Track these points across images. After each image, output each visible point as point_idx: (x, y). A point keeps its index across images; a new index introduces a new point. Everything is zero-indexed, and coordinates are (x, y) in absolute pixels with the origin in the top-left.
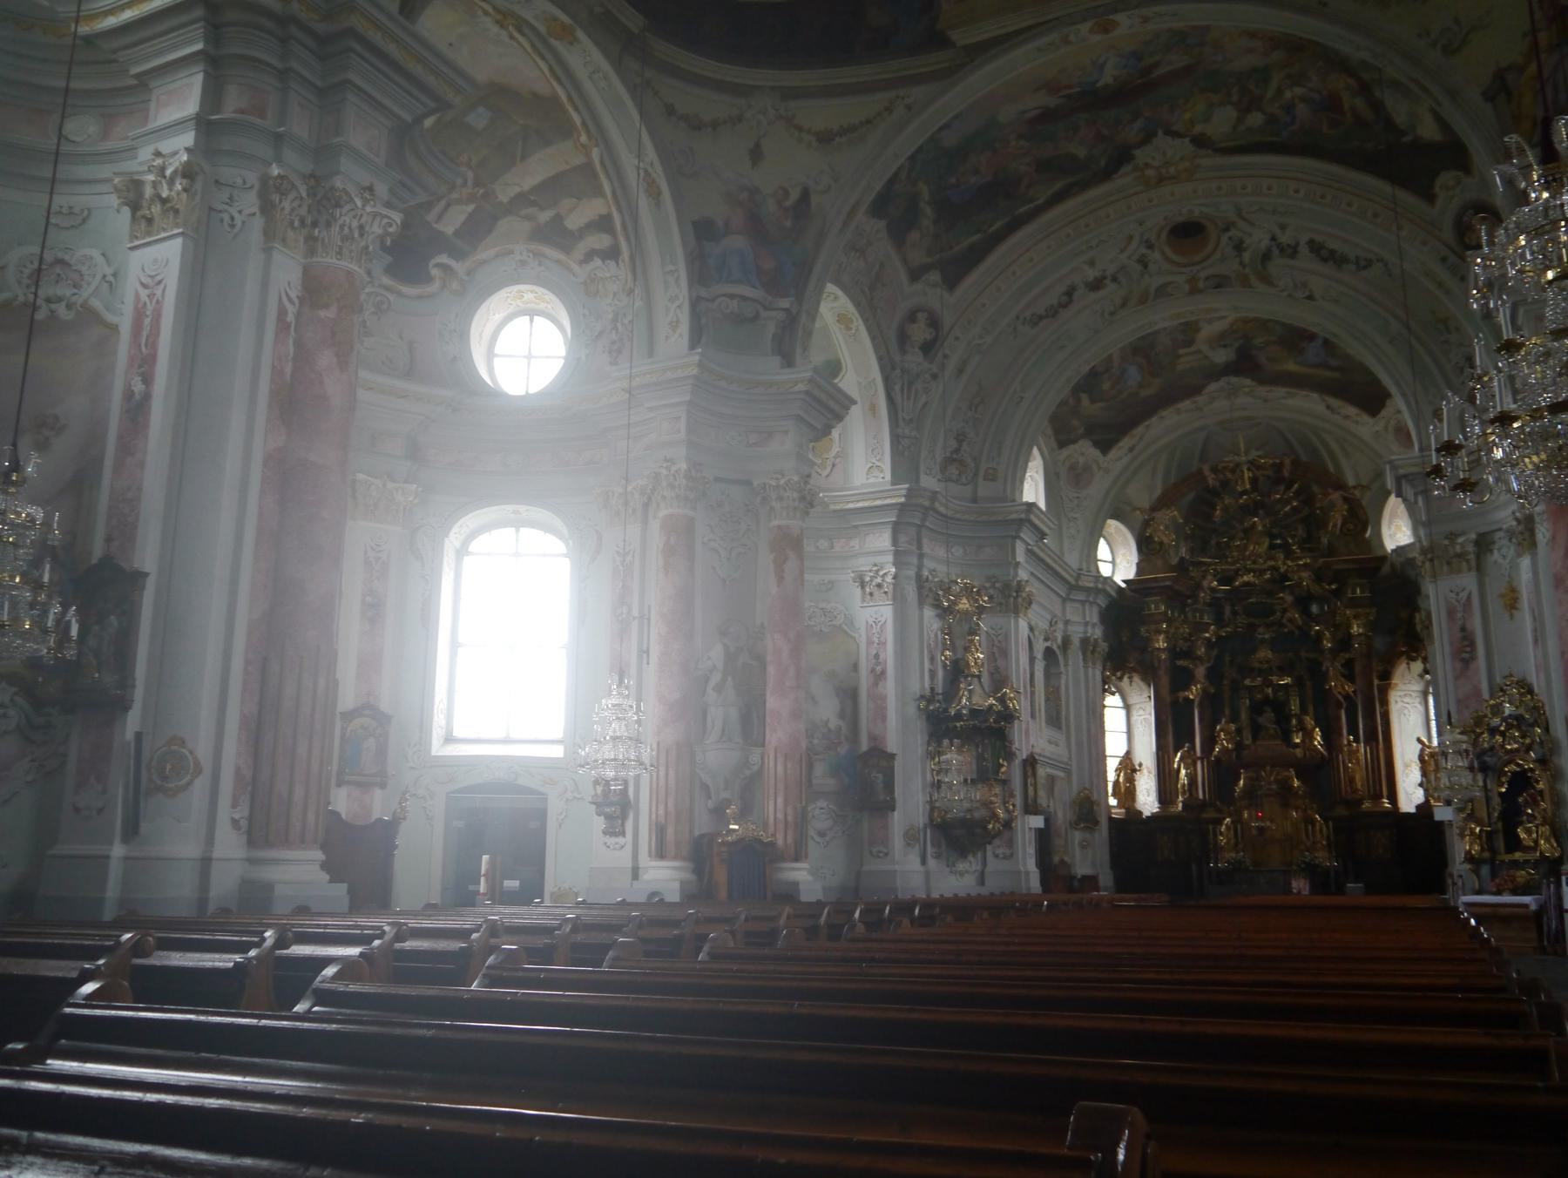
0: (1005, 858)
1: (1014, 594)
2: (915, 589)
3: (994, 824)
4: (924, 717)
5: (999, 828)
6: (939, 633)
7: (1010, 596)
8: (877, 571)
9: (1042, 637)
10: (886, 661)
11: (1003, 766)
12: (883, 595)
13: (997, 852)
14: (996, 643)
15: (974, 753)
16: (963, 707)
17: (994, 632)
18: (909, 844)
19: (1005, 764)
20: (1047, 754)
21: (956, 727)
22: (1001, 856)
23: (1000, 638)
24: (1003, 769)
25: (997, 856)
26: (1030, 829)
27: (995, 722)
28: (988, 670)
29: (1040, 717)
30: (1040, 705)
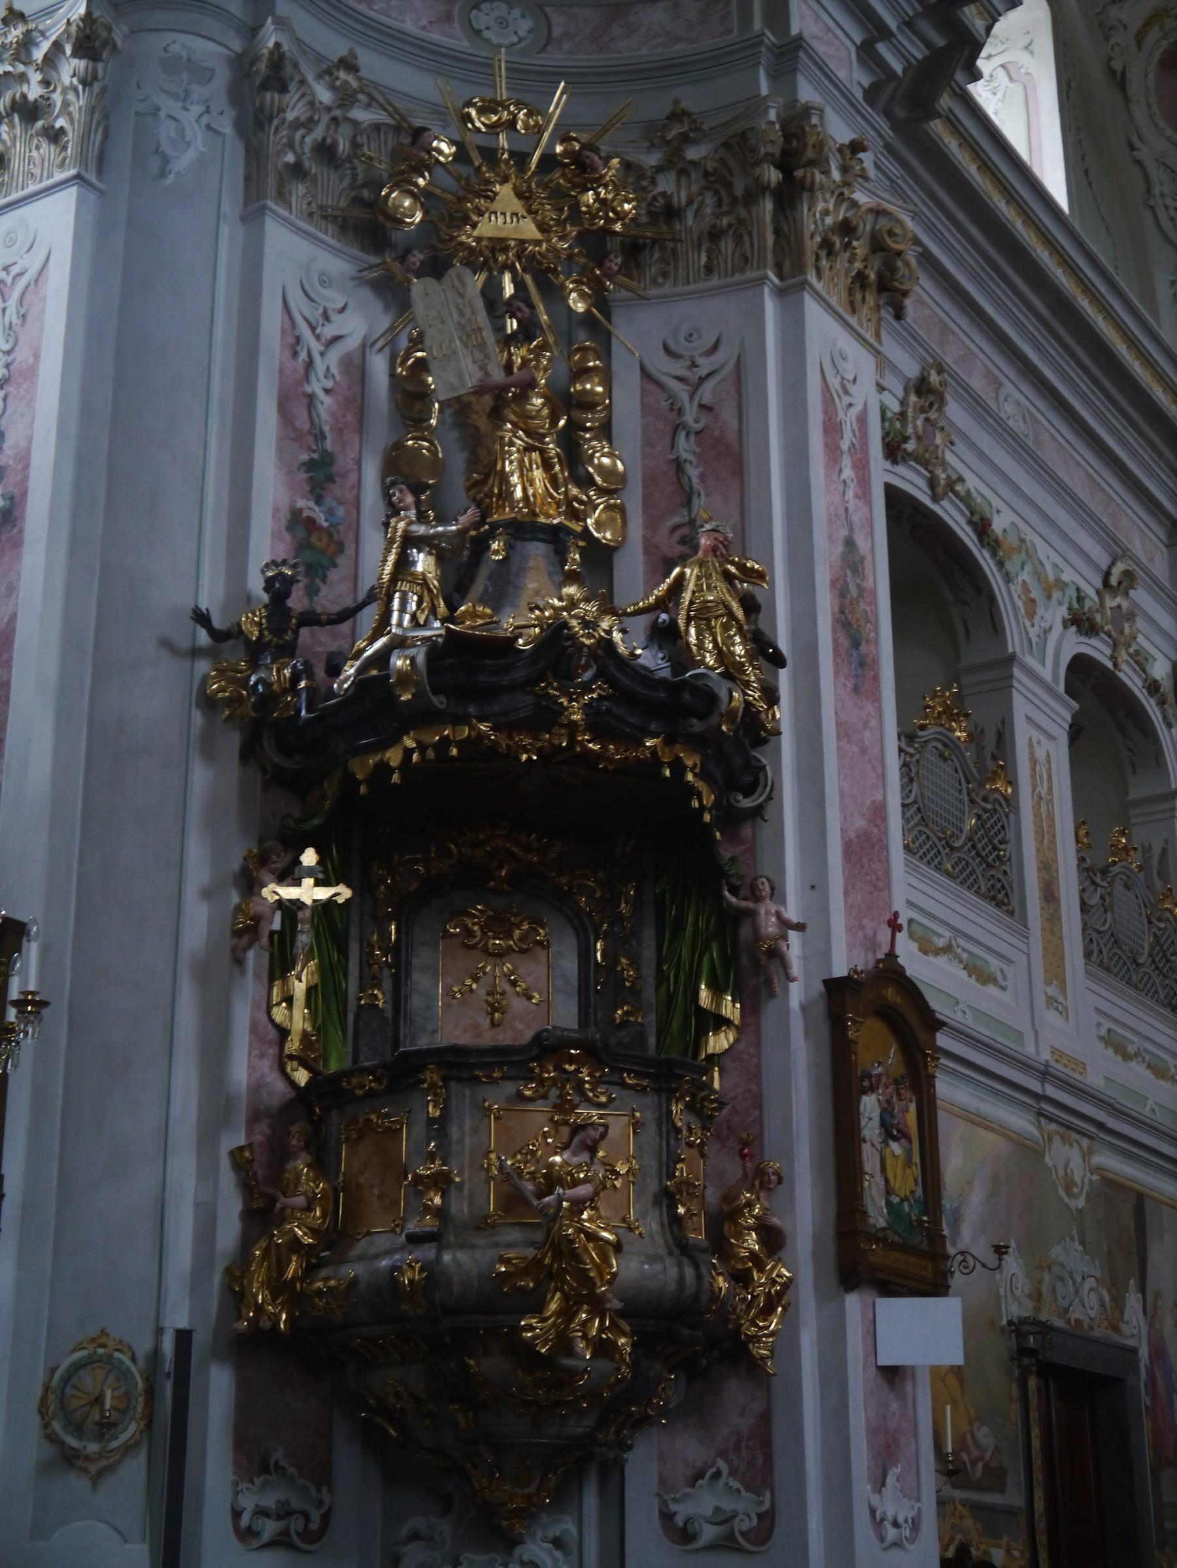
0: (727, 1544)
1: (774, 176)
2: (228, 129)
3: (567, 1313)
4: (232, 742)
5: (603, 1349)
6: (379, 365)
7: (751, 198)
8: (27, 43)
9: (1063, 612)
10: (24, 459)
11: (721, 1022)
12: (47, 149)
13: (681, 1511)
14: (690, 415)
15: (570, 965)
16: (399, 643)
17: (679, 369)
18: (70, 1459)
19: (730, 1008)
20: (1094, 1080)
21: (384, 769)
22: (709, 1533)
23: (707, 393)
24: (718, 1042)
25: (684, 1535)
26: (892, 1375)
27: (597, 724)
28: (649, 548)
29: (1053, 918)
30: (1048, 867)
